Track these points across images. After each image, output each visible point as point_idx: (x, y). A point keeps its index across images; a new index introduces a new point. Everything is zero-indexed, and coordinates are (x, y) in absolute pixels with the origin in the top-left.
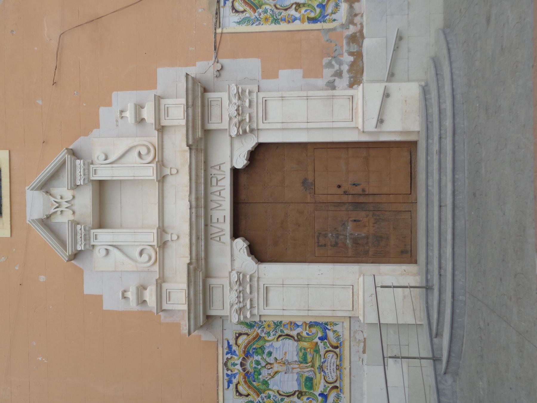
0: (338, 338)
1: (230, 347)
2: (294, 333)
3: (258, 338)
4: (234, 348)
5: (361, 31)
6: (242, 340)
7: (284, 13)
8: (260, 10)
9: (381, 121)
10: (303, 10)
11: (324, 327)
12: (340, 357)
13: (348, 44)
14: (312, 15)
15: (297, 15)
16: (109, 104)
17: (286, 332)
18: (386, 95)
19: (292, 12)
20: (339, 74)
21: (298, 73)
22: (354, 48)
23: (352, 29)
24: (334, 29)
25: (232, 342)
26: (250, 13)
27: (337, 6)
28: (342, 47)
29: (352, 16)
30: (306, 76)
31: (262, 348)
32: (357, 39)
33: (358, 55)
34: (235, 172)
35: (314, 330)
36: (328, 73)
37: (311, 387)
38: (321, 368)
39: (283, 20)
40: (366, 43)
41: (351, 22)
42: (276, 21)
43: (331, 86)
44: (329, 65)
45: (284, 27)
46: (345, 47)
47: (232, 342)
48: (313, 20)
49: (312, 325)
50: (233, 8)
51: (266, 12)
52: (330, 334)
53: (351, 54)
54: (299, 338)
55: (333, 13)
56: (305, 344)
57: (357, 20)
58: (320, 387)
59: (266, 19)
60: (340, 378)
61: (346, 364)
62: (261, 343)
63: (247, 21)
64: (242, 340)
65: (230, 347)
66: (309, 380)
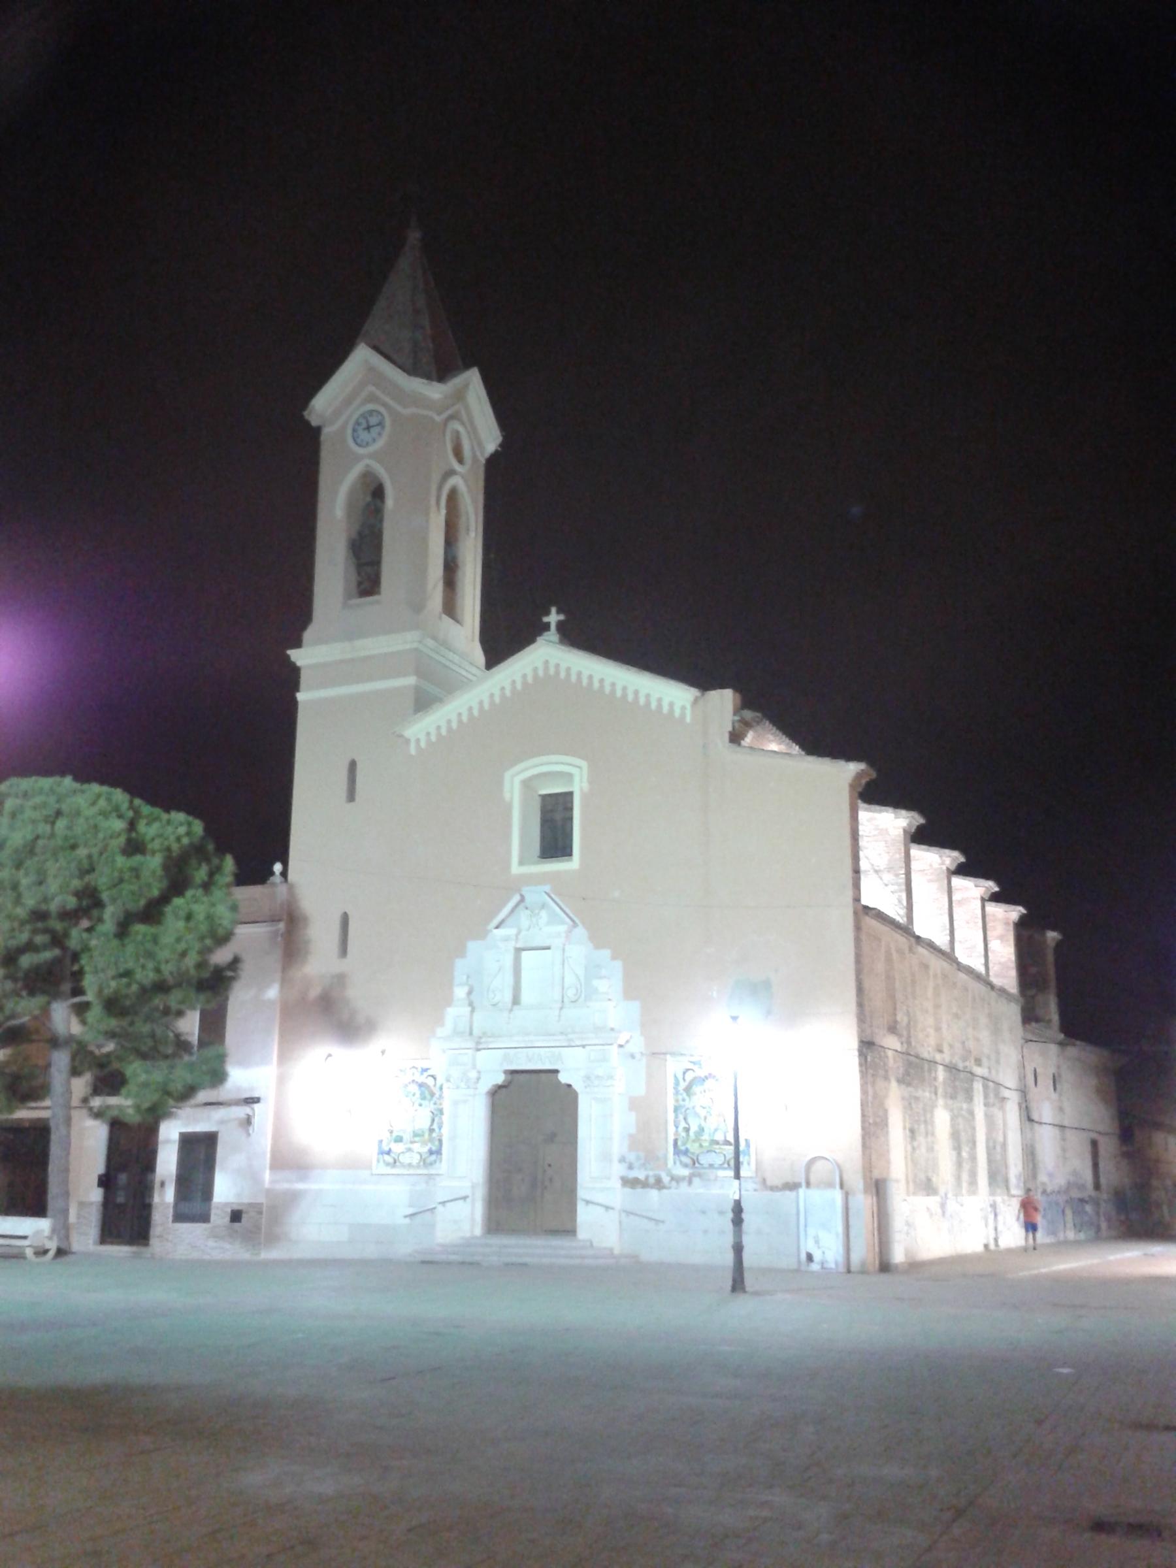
0: (431, 1164)
1: (426, 1070)
2: (435, 1126)
3: (432, 1094)
4: (426, 1074)
5: (664, 1187)
6: (430, 1082)
7: (681, 1117)
8: (685, 1095)
9: (588, 1202)
10: (684, 1134)
11: (439, 1152)
12: (418, 1166)
13: (655, 1176)
14: (679, 1143)
15: (680, 1129)
16: (614, 958)
17: (436, 1119)
18: (607, 1208)
19: (683, 1124)
20: (631, 1167)
21: (633, 1131)
22: (652, 1180)
23: (666, 1179)
24: (666, 1164)
25: (430, 1072)
26: (683, 1085)
27: (686, 1166)
28: (652, 1169)
29: (675, 1179)
30: (631, 1136)
31: (424, 1098)
32: (659, 1184)
33: (645, 1184)
34: (556, 1071)
35: (437, 1143)
36: (631, 1157)
37: (396, 1141)
38: (409, 1150)
39: (676, 1117)
40: (654, 1194)
41: (673, 1178)
42: (676, 1110)
43: (622, 1160)
44: (638, 1158)
45: (671, 1116)
46: (651, 1173)
47: (430, 1072)
48: (676, 1142)
49: (440, 1141)
50: (688, 1070)
51: (684, 1100)
52: (433, 1157)
53: (647, 1178)
54: (431, 1130)
55: (681, 1162)
56: (427, 1136)
57: (674, 1184)
58: (397, 1148)
59: (677, 1101)
60: (403, 1165)
61: (411, 1171)
62: (428, 1097)
63: (677, 1083)
64: (430, 1082)
65: (426, 1070)
66: (399, 1140)
